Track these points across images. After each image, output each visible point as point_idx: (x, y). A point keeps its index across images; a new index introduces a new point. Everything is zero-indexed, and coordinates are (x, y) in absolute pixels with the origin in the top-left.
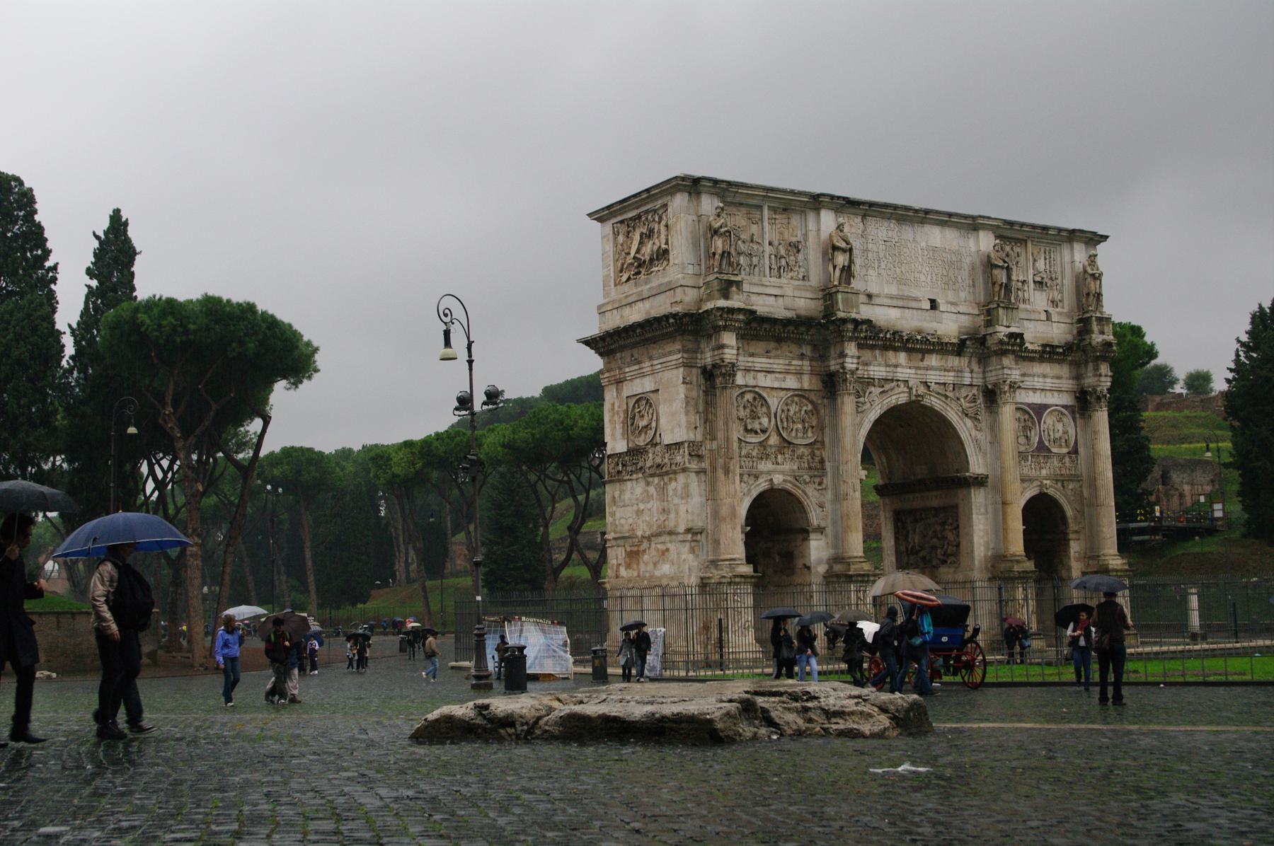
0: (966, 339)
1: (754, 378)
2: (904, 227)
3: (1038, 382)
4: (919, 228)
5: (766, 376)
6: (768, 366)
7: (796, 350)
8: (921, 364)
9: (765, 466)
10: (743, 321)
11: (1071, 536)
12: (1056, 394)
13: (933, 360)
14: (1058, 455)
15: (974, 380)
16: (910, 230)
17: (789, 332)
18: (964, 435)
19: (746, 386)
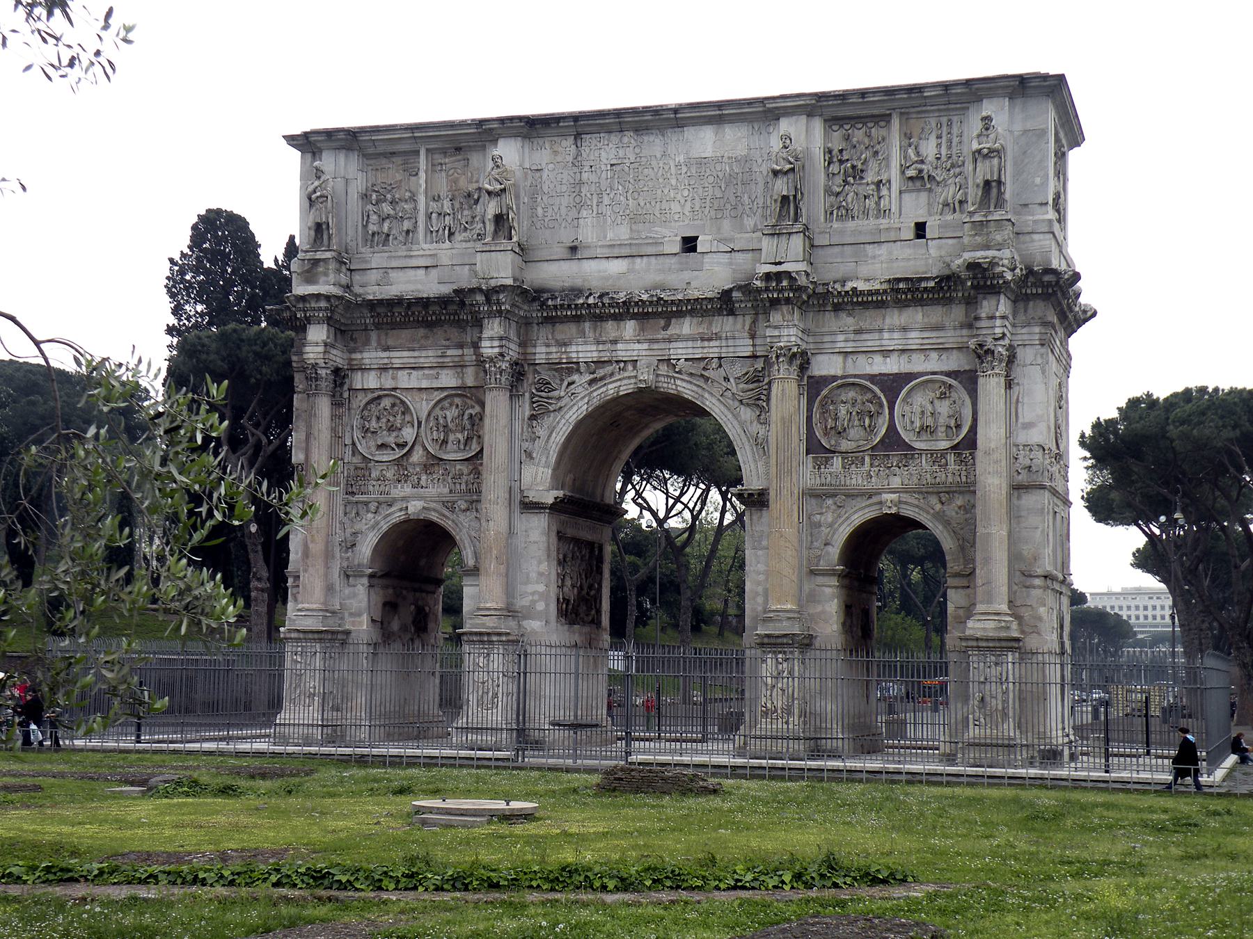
0: (731, 290)
1: (393, 379)
2: (646, 138)
3: (891, 340)
4: (674, 139)
5: (410, 374)
6: (412, 360)
7: (454, 334)
8: (662, 335)
9: (400, 491)
10: (326, 309)
11: (950, 581)
12: (934, 355)
13: (686, 327)
14: (932, 453)
15: (757, 348)
16: (657, 141)
17: (434, 313)
18: (732, 430)
19: (381, 389)
